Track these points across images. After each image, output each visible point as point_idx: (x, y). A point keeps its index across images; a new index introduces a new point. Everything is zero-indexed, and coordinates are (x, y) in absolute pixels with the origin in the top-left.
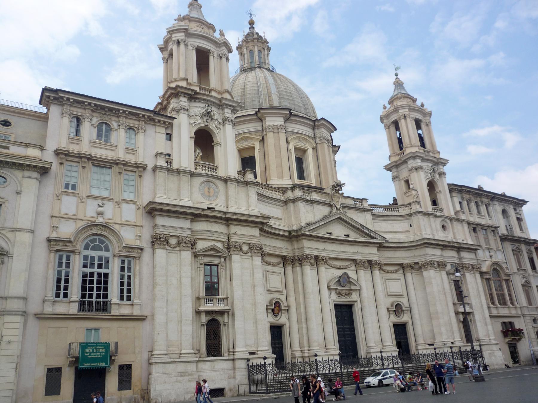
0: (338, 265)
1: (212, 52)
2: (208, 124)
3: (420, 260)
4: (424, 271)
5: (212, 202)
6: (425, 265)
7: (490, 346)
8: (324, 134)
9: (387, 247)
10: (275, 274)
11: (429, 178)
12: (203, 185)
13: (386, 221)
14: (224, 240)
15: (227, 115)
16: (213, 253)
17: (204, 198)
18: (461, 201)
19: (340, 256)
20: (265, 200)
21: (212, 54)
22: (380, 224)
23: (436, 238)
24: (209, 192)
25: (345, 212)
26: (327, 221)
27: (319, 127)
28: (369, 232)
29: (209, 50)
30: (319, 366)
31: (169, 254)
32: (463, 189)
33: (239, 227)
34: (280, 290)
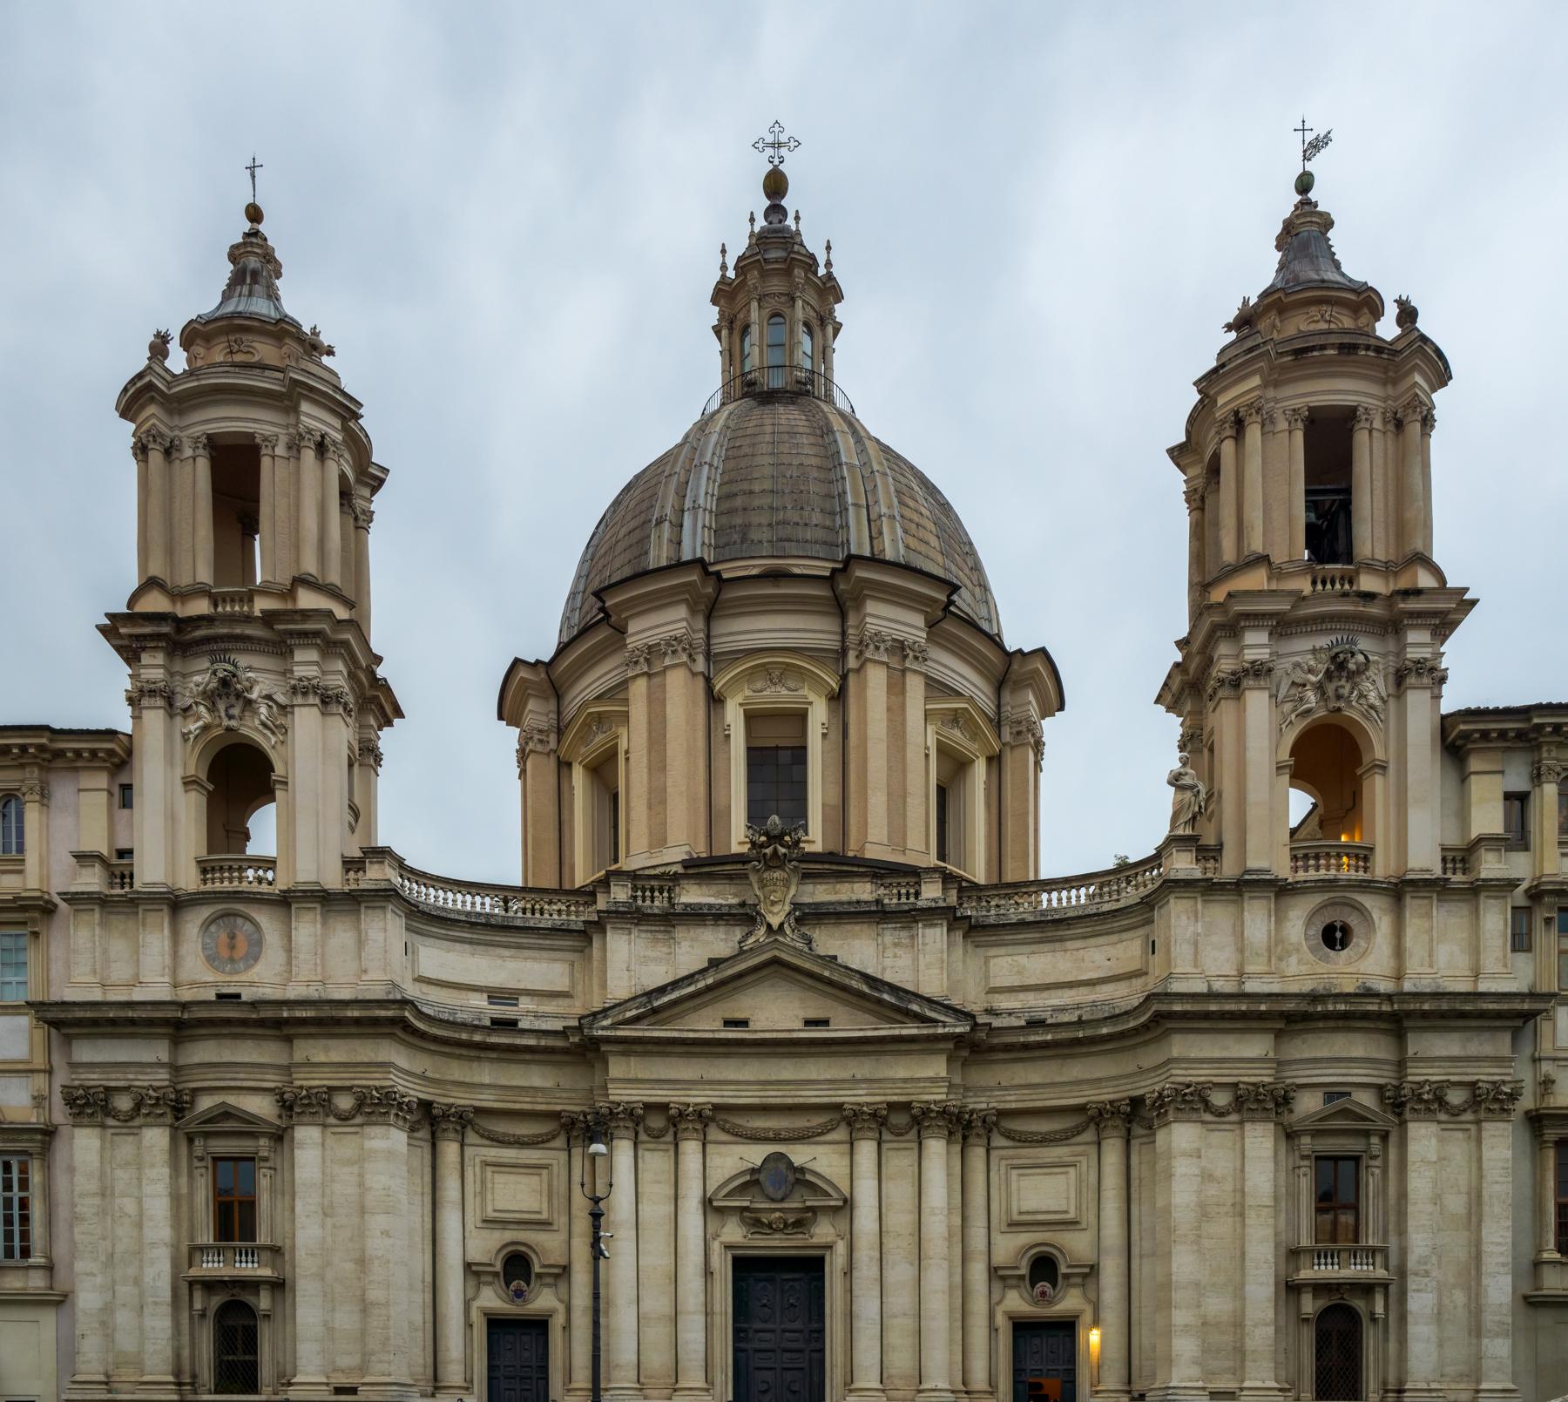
3: (1147, 1087)
4: (1160, 1127)
5: (235, 978)
6: (1161, 1106)
8: (872, 625)
9: (1026, 1047)
12: (213, 928)
13: (1057, 945)
14: (272, 1085)
17: (217, 969)
19: (774, 1096)
25: (804, 936)
26: (710, 981)
28: (900, 999)
31: (115, 1138)
33: (323, 1042)
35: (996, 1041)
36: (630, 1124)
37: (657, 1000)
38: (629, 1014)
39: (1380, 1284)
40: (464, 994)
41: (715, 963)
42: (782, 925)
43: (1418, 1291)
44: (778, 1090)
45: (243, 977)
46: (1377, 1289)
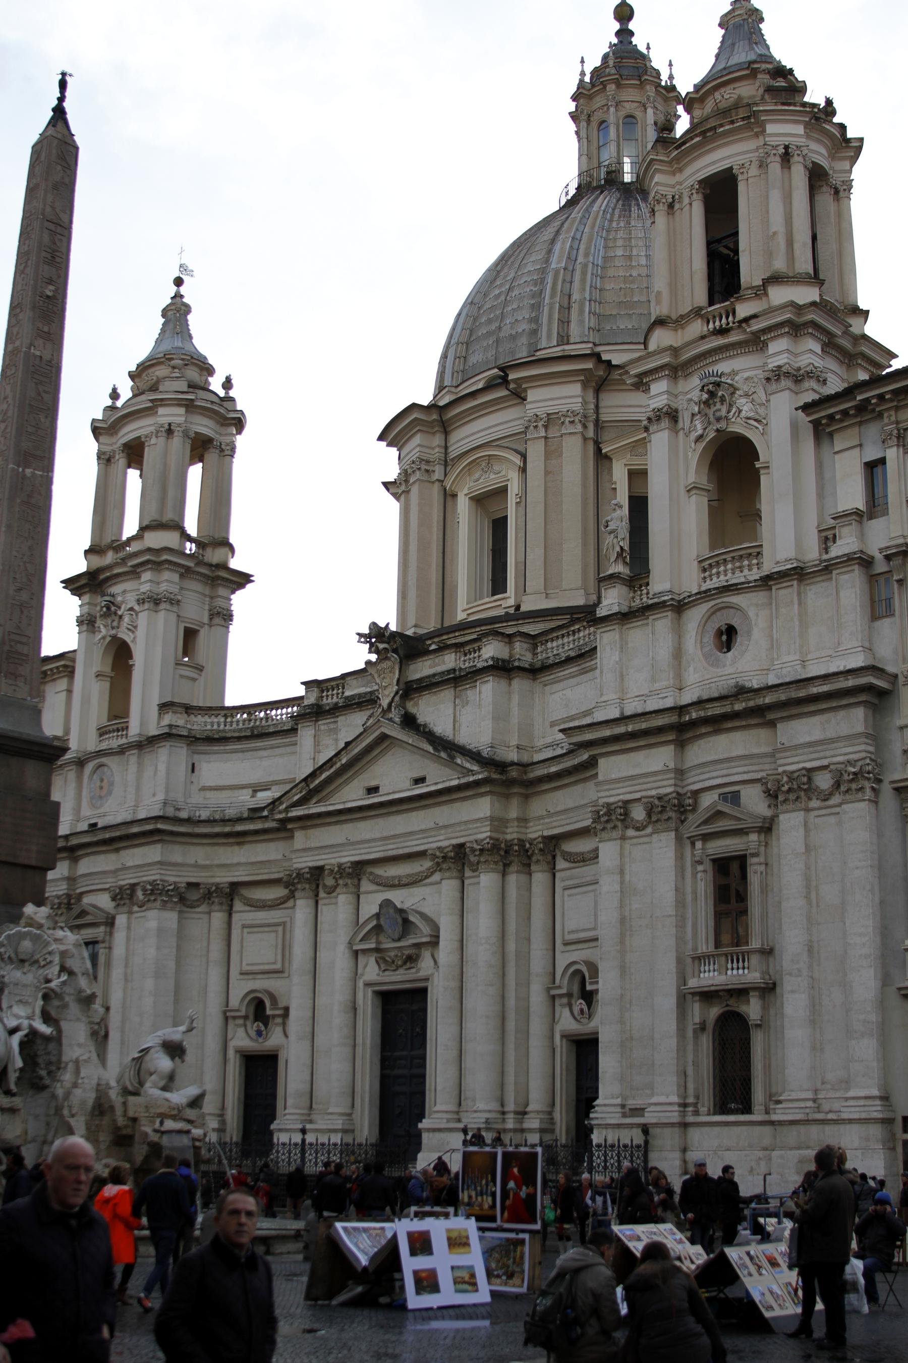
0: (393, 878)
1: (146, 437)
2: (114, 632)
7: (828, 1128)
10: (266, 929)
11: (700, 438)
12: (95, 777)
15: (145, 588)
16: (88, 919)
18: (872, 454)
19: (392, 849)
20: (258, 744)
21: (146, 444)
22: (568, 692)
23: (653, 705)
24: (101, 788)
26: (344, 761)
27: (525, 390)
29: (139, 437)
30: (594, 1158)
32: (867, 400)
34: (278, 966)
35: (531, 775)
36: (307, 886)
37: (312, 782)
38: (296, 798)
39: (755, 989)
40: (236, 793)
41: (348, 744)
42: (390, 705)
43: (793, 992)
44: (394, 843)
45: (102, 810)
46: (751, 994)
